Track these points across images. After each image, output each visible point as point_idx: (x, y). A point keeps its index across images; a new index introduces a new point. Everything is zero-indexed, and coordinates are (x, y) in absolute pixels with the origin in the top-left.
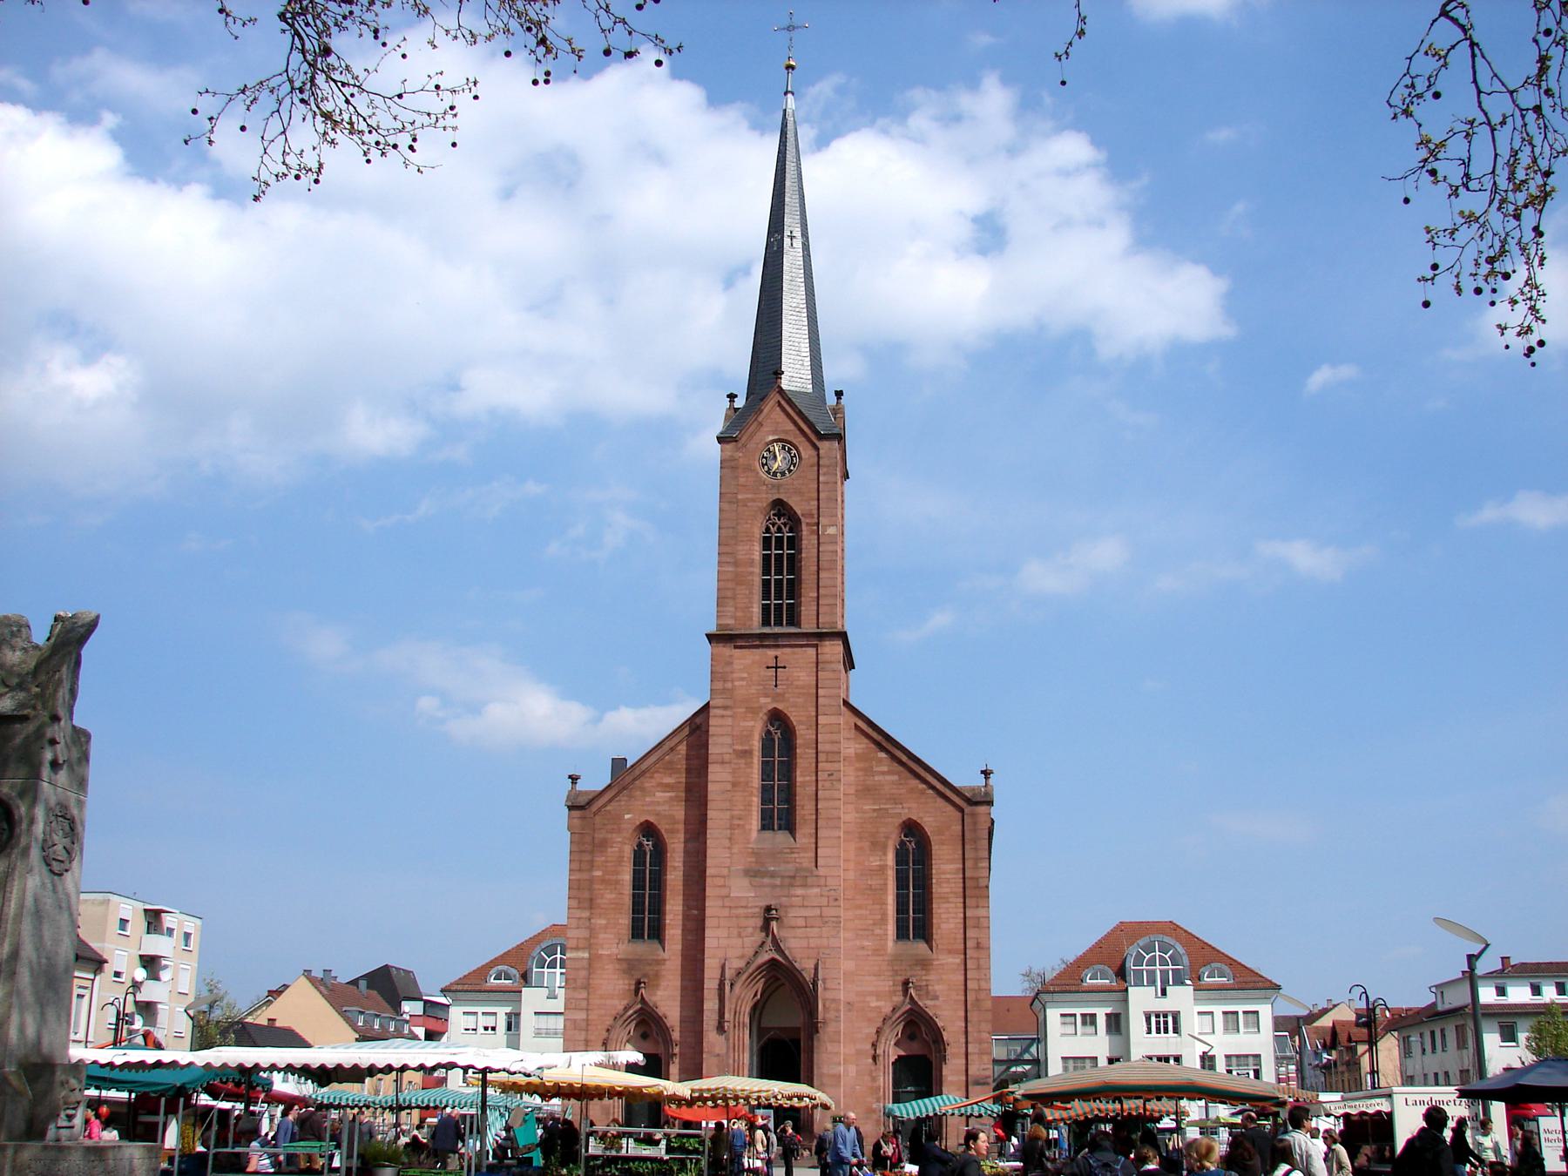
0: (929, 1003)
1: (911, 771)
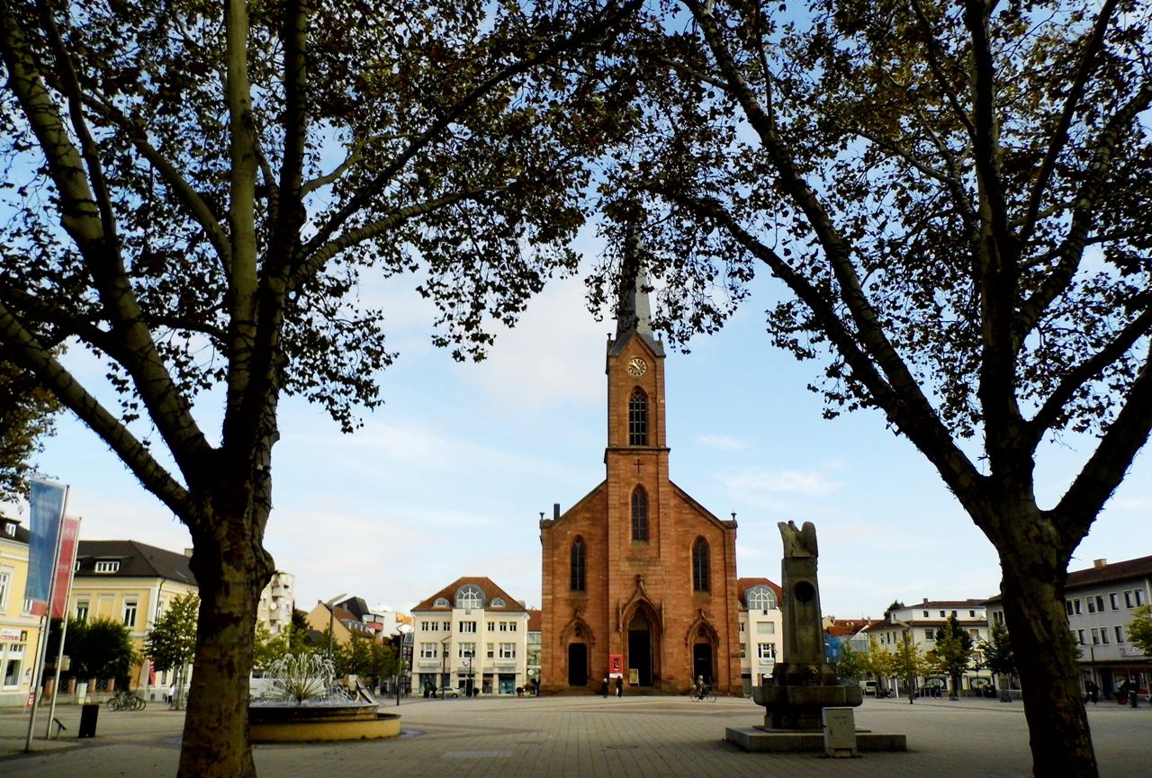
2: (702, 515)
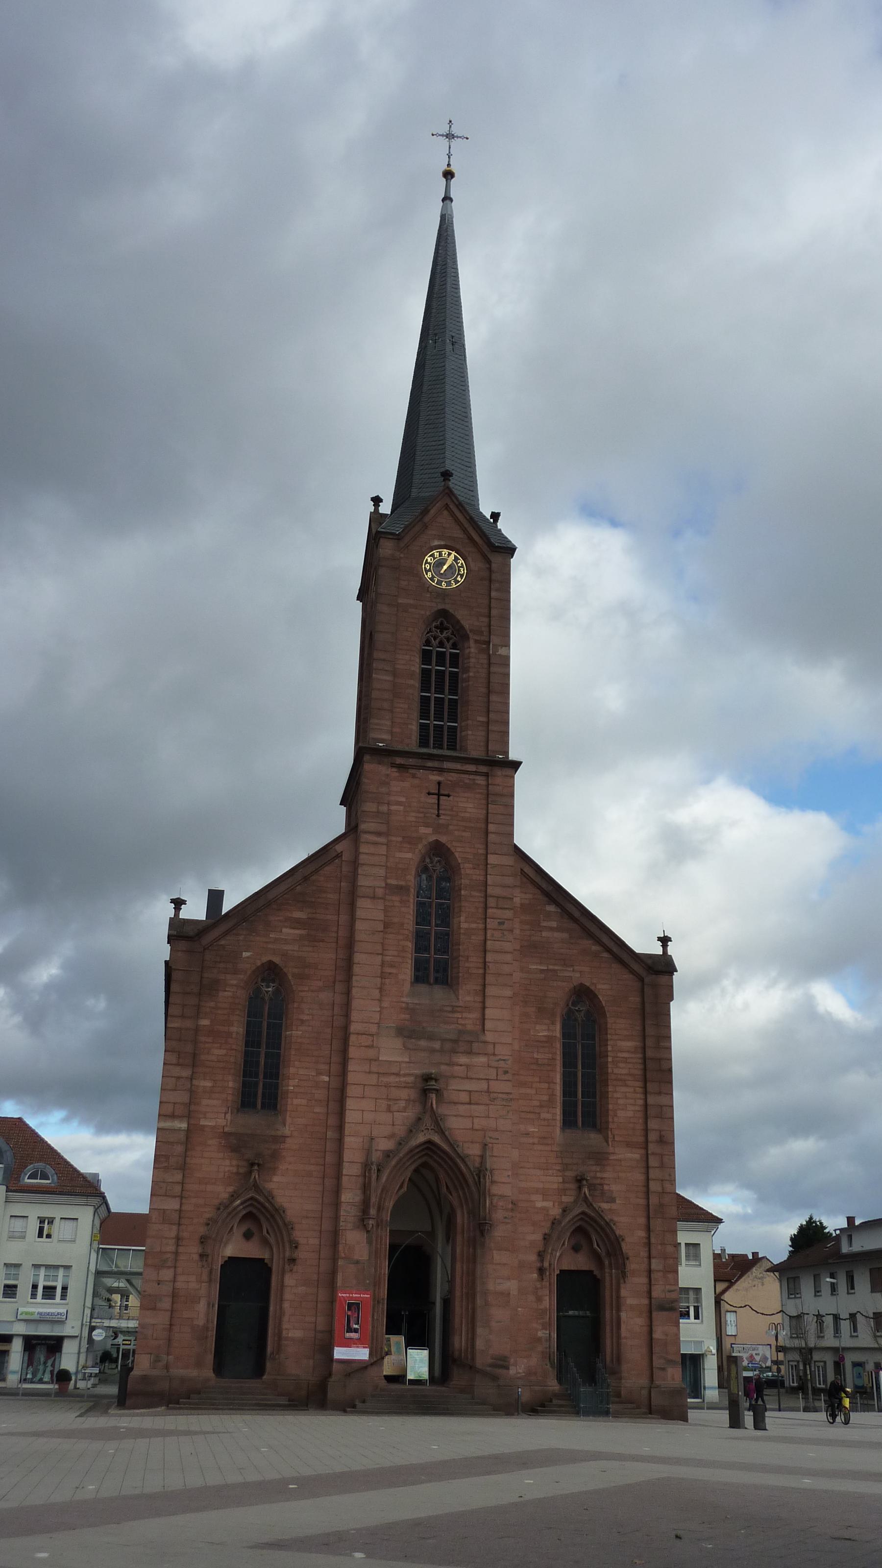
0: (605, 1206)
1: (584, 929)
2: (591, 935)
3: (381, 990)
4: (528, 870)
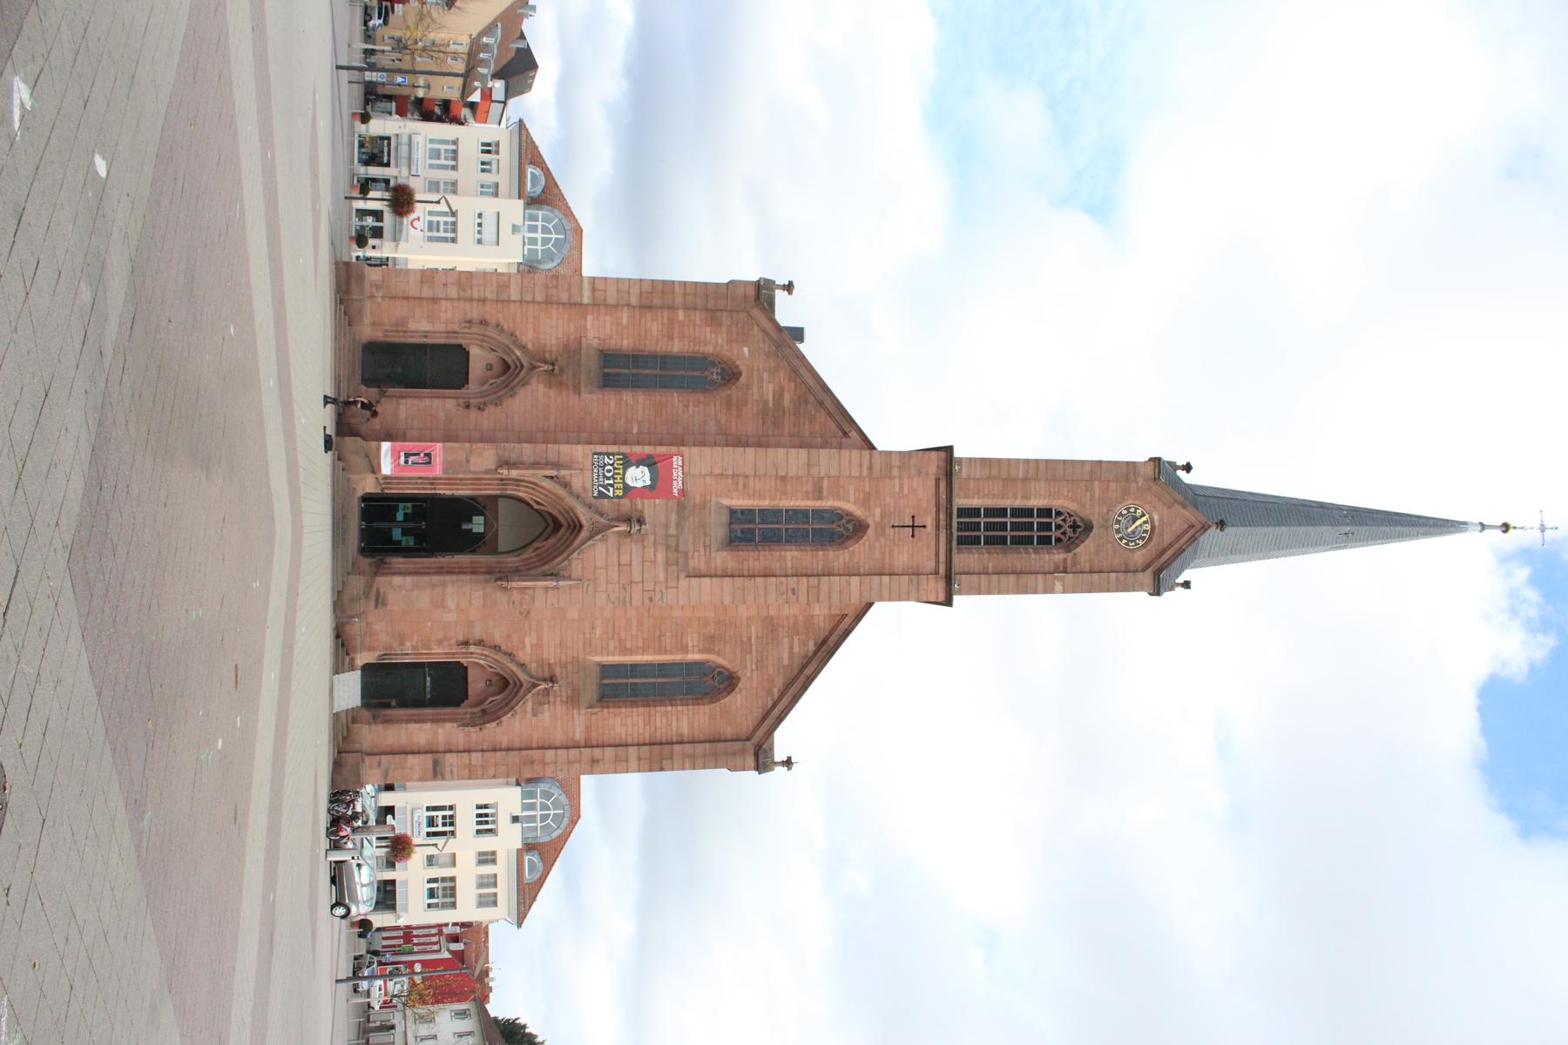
0: (529, 706)
3: (722, 475)
4: (847, 621)
